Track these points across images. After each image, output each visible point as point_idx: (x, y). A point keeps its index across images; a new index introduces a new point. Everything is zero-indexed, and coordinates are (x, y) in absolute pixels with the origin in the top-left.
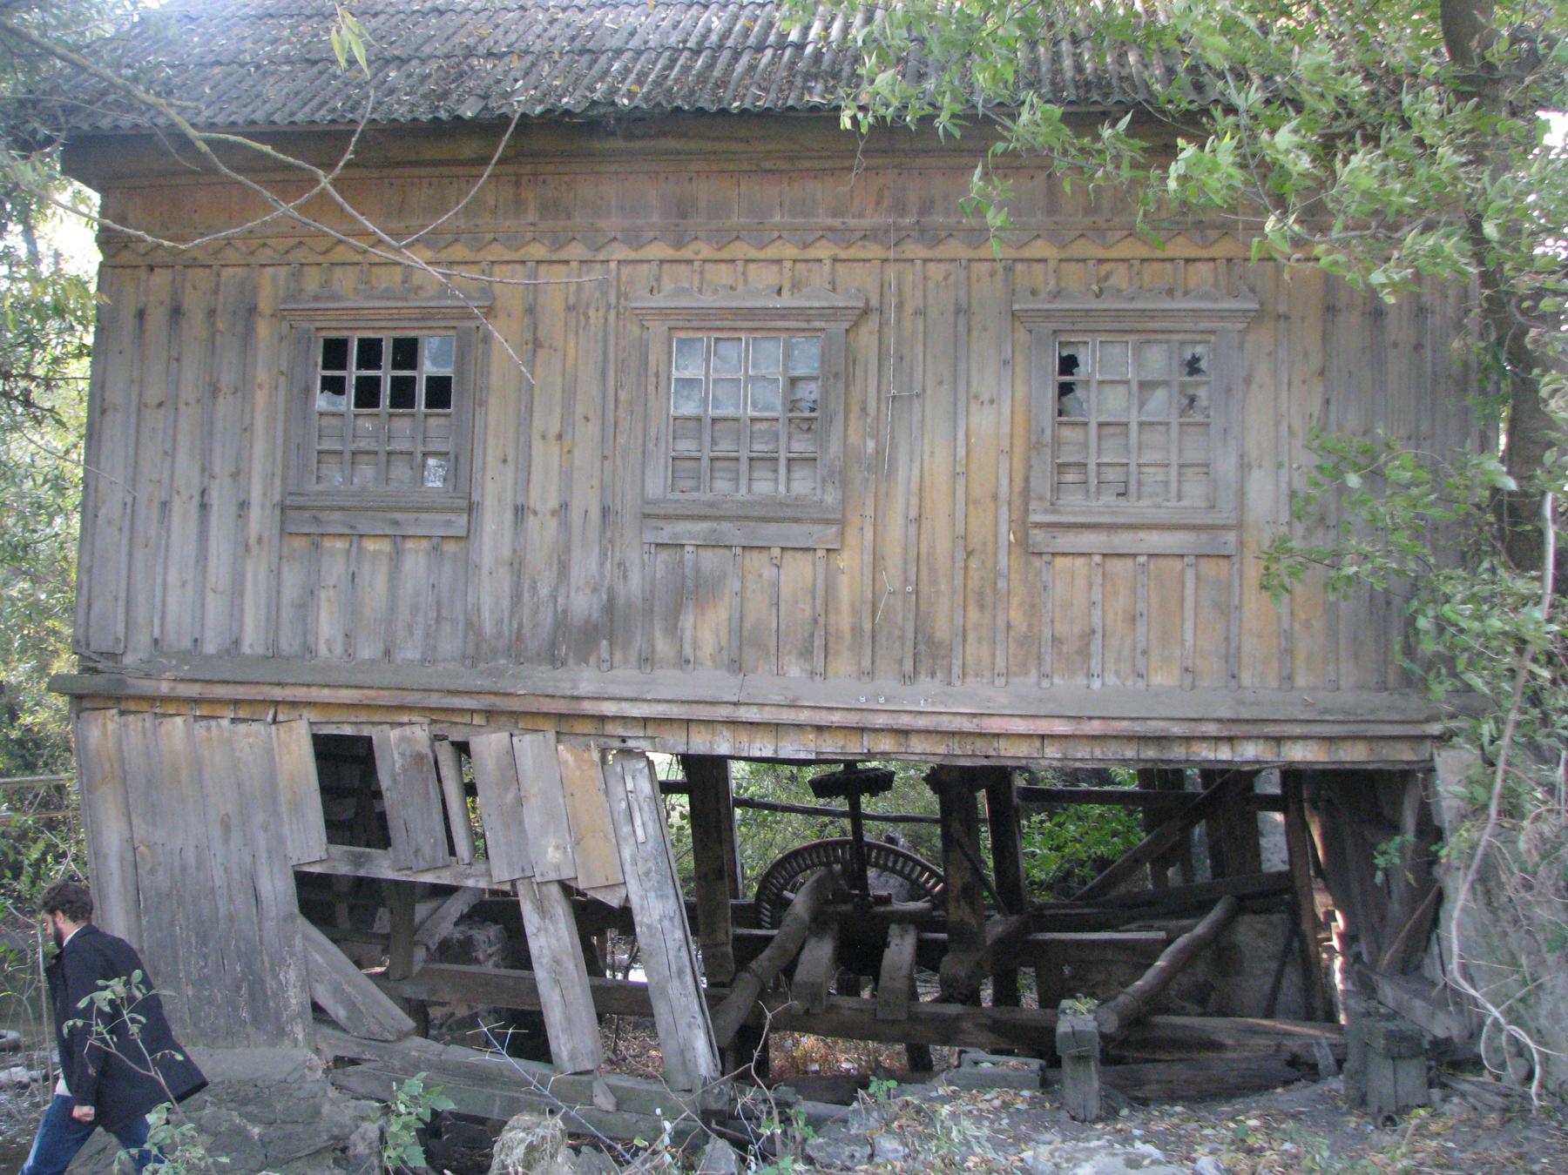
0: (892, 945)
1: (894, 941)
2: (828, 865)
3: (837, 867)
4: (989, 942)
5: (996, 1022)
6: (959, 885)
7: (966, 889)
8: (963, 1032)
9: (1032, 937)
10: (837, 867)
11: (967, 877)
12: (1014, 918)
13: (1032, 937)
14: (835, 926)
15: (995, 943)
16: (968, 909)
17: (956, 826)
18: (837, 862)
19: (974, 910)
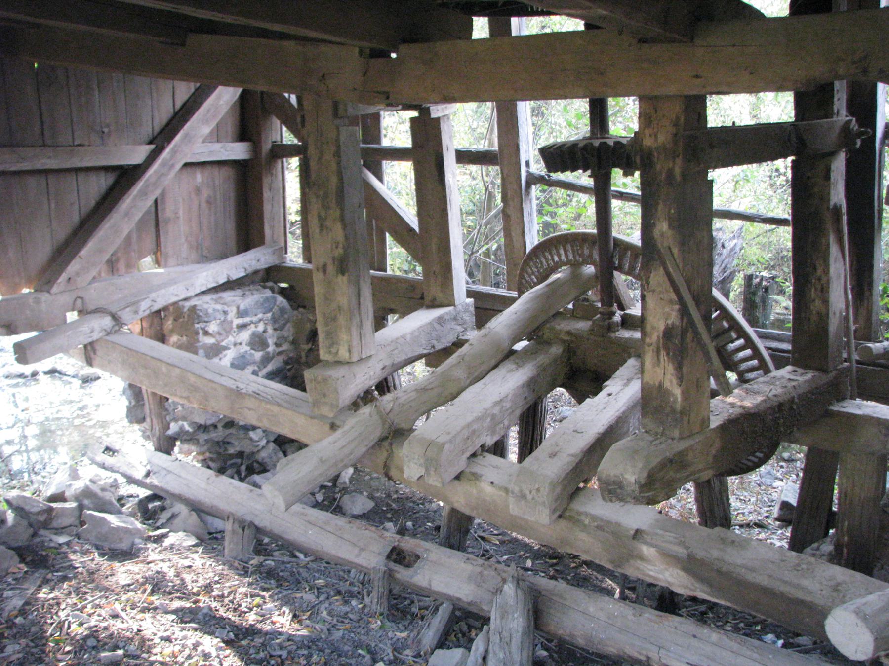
0: (602, 394)
1: (612, 386)
2: (576, 266)
3: (590, 270)
4: (715, 422)
5: (691, 558)
6: (662, 328)
7: (668, 333)
8: (641, 558)
9: (836, 407)
10: (590, 270)
11: (674, 318)
12: (809, 375)
13: (836, 407)
14: (556, 350)
15: (723, 427)
16: (670, 368)
17: (662, 227)
18: (585, 263)
19: (679, 367)
